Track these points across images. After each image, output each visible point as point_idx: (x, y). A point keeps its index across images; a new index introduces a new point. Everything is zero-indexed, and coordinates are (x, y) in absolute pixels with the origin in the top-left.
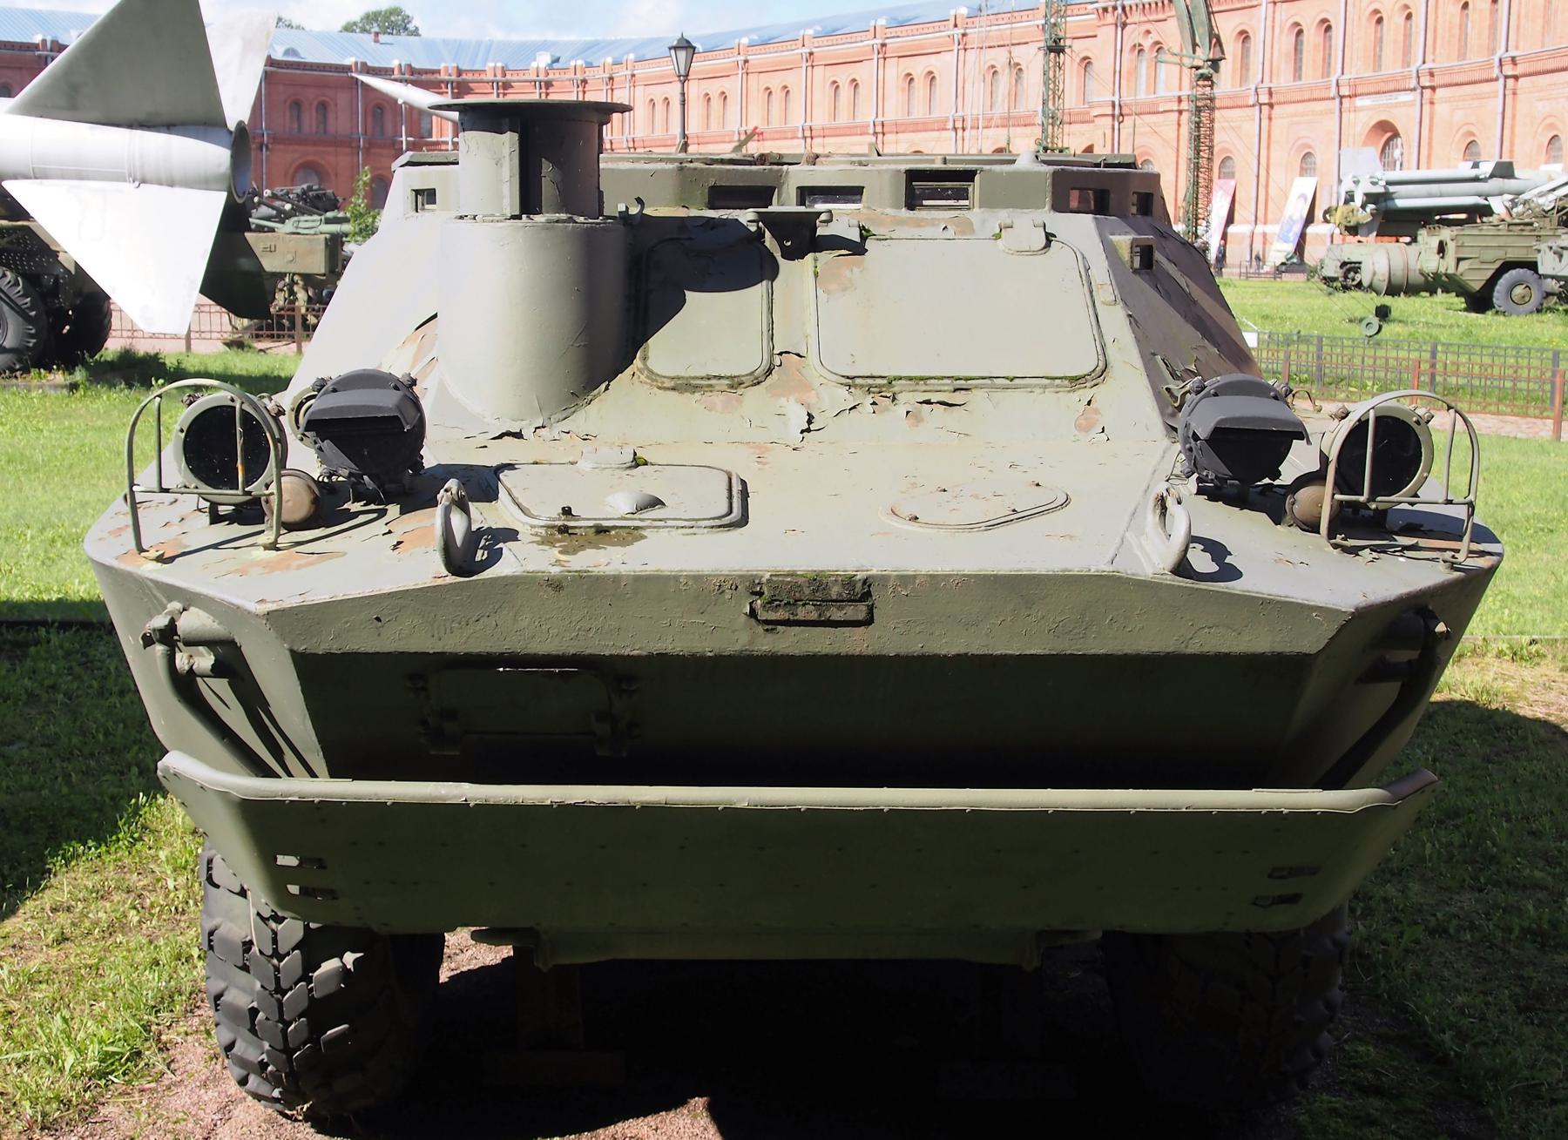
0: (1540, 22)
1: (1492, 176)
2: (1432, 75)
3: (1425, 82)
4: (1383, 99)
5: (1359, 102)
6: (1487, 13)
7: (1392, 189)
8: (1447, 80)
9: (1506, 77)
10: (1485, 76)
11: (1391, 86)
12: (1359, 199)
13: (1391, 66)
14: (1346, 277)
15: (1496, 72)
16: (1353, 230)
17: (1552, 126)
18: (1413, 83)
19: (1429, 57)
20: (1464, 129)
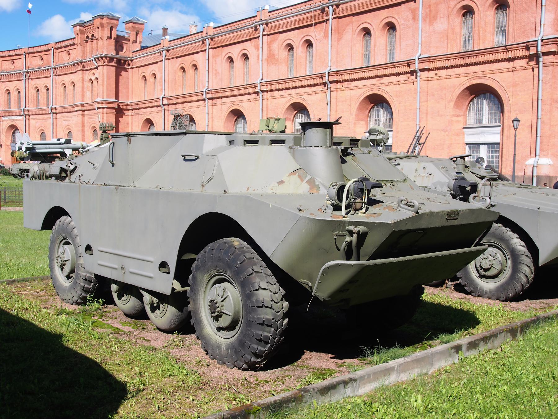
0: (63, 97)
1: (64, 143)
2: (28, 111)
3: (26, 113)
4: (13, 118)
7: (35, 146)
8: (34, 113)
9: (53, 113)
10: (46, 112)
11: (14, 114)
13: (14, 107)
14: (21, 174)
15: (50, 112)
16: (22, 159)
17: (68, 129)
18: (22, 113)
19: (27, 105)
20: (40, 128)
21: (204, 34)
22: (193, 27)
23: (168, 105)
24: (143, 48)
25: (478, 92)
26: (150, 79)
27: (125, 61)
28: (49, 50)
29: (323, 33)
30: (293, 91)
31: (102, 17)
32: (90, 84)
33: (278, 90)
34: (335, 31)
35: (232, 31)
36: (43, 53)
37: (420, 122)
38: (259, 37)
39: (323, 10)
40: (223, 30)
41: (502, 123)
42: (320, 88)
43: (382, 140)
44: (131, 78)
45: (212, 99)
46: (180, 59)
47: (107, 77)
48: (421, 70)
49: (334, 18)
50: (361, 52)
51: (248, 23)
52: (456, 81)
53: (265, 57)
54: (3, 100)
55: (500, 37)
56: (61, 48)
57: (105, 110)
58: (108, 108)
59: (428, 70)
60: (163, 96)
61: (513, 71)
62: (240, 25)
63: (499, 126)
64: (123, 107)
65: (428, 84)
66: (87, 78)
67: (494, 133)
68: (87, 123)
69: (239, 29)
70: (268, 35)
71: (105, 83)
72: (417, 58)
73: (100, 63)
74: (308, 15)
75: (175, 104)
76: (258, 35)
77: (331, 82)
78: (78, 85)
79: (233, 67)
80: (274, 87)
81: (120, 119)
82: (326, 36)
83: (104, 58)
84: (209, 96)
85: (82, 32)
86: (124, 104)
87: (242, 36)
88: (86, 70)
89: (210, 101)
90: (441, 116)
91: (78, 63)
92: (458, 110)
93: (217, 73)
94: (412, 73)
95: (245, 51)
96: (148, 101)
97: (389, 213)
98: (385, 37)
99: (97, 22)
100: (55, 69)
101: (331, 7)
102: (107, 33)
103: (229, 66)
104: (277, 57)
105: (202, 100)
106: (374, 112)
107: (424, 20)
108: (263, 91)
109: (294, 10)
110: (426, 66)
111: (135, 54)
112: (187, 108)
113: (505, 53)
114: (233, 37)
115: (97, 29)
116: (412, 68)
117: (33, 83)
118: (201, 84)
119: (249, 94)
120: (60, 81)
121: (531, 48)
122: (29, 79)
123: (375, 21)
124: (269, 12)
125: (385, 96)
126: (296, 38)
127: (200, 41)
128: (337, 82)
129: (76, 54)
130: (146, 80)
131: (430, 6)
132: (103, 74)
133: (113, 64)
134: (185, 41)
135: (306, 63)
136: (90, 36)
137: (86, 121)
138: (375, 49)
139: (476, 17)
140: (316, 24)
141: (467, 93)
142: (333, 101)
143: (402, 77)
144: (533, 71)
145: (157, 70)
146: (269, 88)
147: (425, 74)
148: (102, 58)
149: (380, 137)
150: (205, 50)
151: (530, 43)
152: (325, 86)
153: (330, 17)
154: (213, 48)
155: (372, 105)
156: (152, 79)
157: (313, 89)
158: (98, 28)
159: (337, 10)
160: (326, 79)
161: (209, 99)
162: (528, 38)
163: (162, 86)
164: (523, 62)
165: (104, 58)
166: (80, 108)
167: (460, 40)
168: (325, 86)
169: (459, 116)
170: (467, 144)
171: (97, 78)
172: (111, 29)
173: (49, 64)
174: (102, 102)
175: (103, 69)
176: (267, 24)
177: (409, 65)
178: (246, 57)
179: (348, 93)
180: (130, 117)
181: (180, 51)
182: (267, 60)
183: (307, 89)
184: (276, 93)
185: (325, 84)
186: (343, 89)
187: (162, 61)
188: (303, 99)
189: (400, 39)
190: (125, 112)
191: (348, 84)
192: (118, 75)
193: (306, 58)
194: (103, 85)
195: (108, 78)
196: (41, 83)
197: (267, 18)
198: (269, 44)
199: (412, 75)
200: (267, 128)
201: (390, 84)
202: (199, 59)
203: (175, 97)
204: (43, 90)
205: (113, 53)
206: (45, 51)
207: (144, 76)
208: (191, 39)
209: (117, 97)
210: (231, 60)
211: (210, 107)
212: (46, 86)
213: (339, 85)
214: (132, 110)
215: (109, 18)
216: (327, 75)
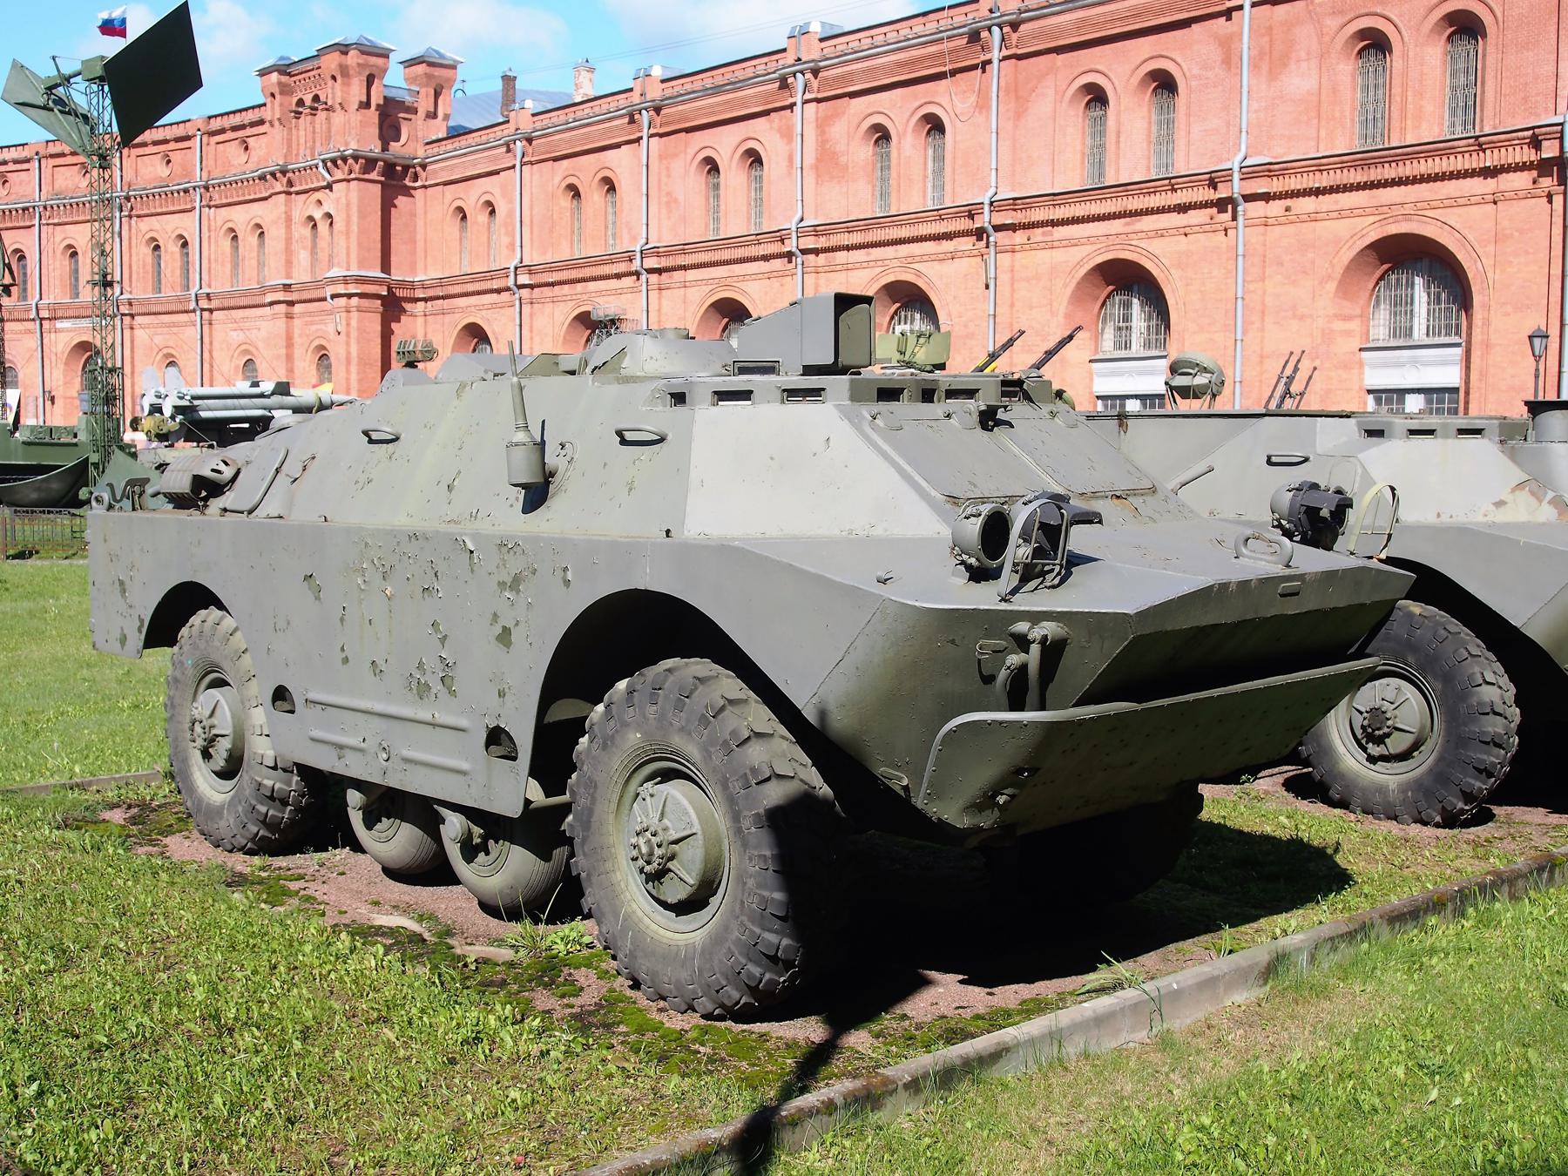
0: (228, 266)
2: (130, 304)
5: (59, 325)
6: (178, 256)
8: (144, 310)
12: (168, 411)
15: (192, 305)
17: (246, 352)
21: (635, 98)
22: (584, 73)
23: (531, 287)
24: (457, 133)
25: (1405, 256)
26: (478, 217)
27: (406, 168)
28: (188, 138)
29: (973, 98)
30: (889, 252)
31: (343, 49)
32: (307, 231)
33: (848, 248)
34: (1007, 92)
35: (717, 90)
36: (172, 146)
37: (1245, 332)
38: (791, 106)
39: (974, 37)
40: (689, 87)
41: (1464, 335)
42: (966, 243)
43: (1207, 386)
44: (425, 212)
45: (659, 271)
46: (565, 163)
47: (360, 211)
48: (1249, 198)
49: (1006, 58)
50: (1079, 148)
51: (761, 69)
52: (1343, 227)
53: (810, 159)
54: (58, 273)
55: (1460, 112)
56: (222, 131)
57: (355, 300)
58: (362, 296)
59: (1267, 197)
60: (516, 262)
61: (1495, 203)
62: (739, 72)
63: (1458, 345)
64: (400, 293)
65: (1264, 234)
66: (299, 214)
67: (1444, 363)
68: (301, 336)
69: (737, 85)
70: (818, 101)
71: (355, 228)
72: (1236, 168)
73: (339, 175)
74: (932, 49)
75: (552, 284)
76: (791, 100)
77: (997, 228)
78: (275, 234)
79: (717, 187)
80: (835, 240)
81: (394, 325)
82: (982, 105)
83: (351, 161)
84: (651, 263)
85: (285, 90)
86: (403, 284)
87: (744, 102)
88: (298, 193)
89: (654, 278)
90: (1302, 318)
91: (273, 175)
92: (1346, 303)
93: (671, 202)
94: (1221, 205)
95: (752, 144)
96: (473, 277)
97: (1130, 575)
98: (1145, 109)
99: (331, 62)
100: (207, 188)
101: (996, 29)
102: (357, 92)
103: (707, 183)
104: (843, 159)
105: (630, 274)
106: (1115, 309)
107: (1255, 66)
108: (804, 252)
109: (892, 36)
110: (1260, 186)
111: (435, 149)
112: (585, 297)
113: (1474, 156)
114: (718, 104)
115: (330, 82)
116: (1223, 193)
117: (145, 225)
118: (625, 232)
119: (766, 258)
120: (219, 223)
121: (1544, 144)
122: (130, 217)
123: (1120, 69)
124: (822, 40)
125: (1148, 265)
126: (899, 110)
127: (622, 116)
128: (1013, 228)
129: (268, 150)
130: (464, 217)
131: (1270, 28)
132: (348, 205)
133: (374, 176)
134: (579, 114)
135: (925, 177)
136: (308, 99)
137: (297, 332)
138: (1118, 142)
139: (1396, 60)
140: (954, 73)
141: (1372, 258)
142: (1004, 278)
143: (1195, 217)
144: (1550, 202)
145: (497, 191)
146: (822, 242)
147: (1257, 208)
148: (345, 159)
149: (1201, 380)
150: (639, 140)
151: (1544, 130)
152: (980, 239)
153: (995, 55)
154: (661, 135)
155: (1111, 288)
156: (483, 218)
157: (947, 246)
158: (334, 78)
159: (1014, 36)
160: (984, 220)
161: (650, 271)
162: (1537, 115)
163: (513, 236)
164: (1522, 180)
165: (351, 161)
166: (280, 296)
167: (1352, 120)
168: (980, 239)
169: (1349, 318)
170: (1369, 392)
171: (329, 216)
172: (370, 80)
173: (188, 172)
174: (345, 280)
175: (348, 189)
176: (815, 72)
177: (1213, 184)
178: (754, 158)
179: (1045, 256)
180: (420, 320)
181: (564, 142)
182: (816, 168)
183: (929, 247)
184: (841, 256)
185: (980, 233)
186: (1031, 246)
187: (513, 167)
188: (919, 273)
189: (1188, 115)
190: (408, 306)
191: (1044, 234)
192: (387, 206)
193: (925, 164)
194: (348, 233)
195: (362, 215)
196: (167, 228)
197: (816, 55)
198: (822, 125)
199: (1222, 210)
200: (898, 356)
201: (1160, 234)
202: (620, 162)
203: (551, 267)
204: (171, 249)
205: (373, 147)
206: (178, 140)
207: (460, 209)
208: (597, 110)
209: (386, 266)
210: (712, 166)
211: (653, 295)
212: (181, 237)
213: (1020, 237)
214: (425, 300)
215: (363, 53)
216: (987, 208)
